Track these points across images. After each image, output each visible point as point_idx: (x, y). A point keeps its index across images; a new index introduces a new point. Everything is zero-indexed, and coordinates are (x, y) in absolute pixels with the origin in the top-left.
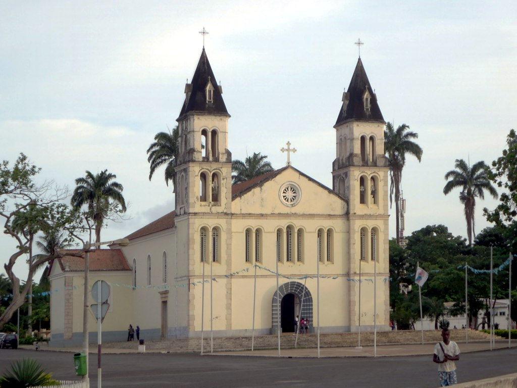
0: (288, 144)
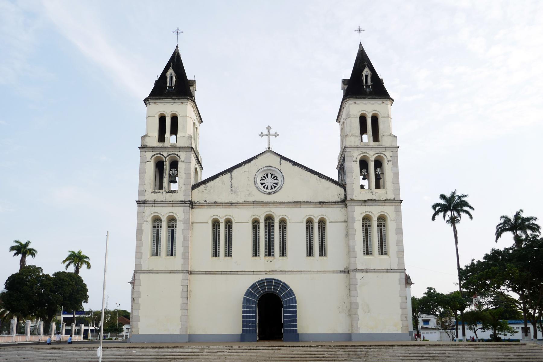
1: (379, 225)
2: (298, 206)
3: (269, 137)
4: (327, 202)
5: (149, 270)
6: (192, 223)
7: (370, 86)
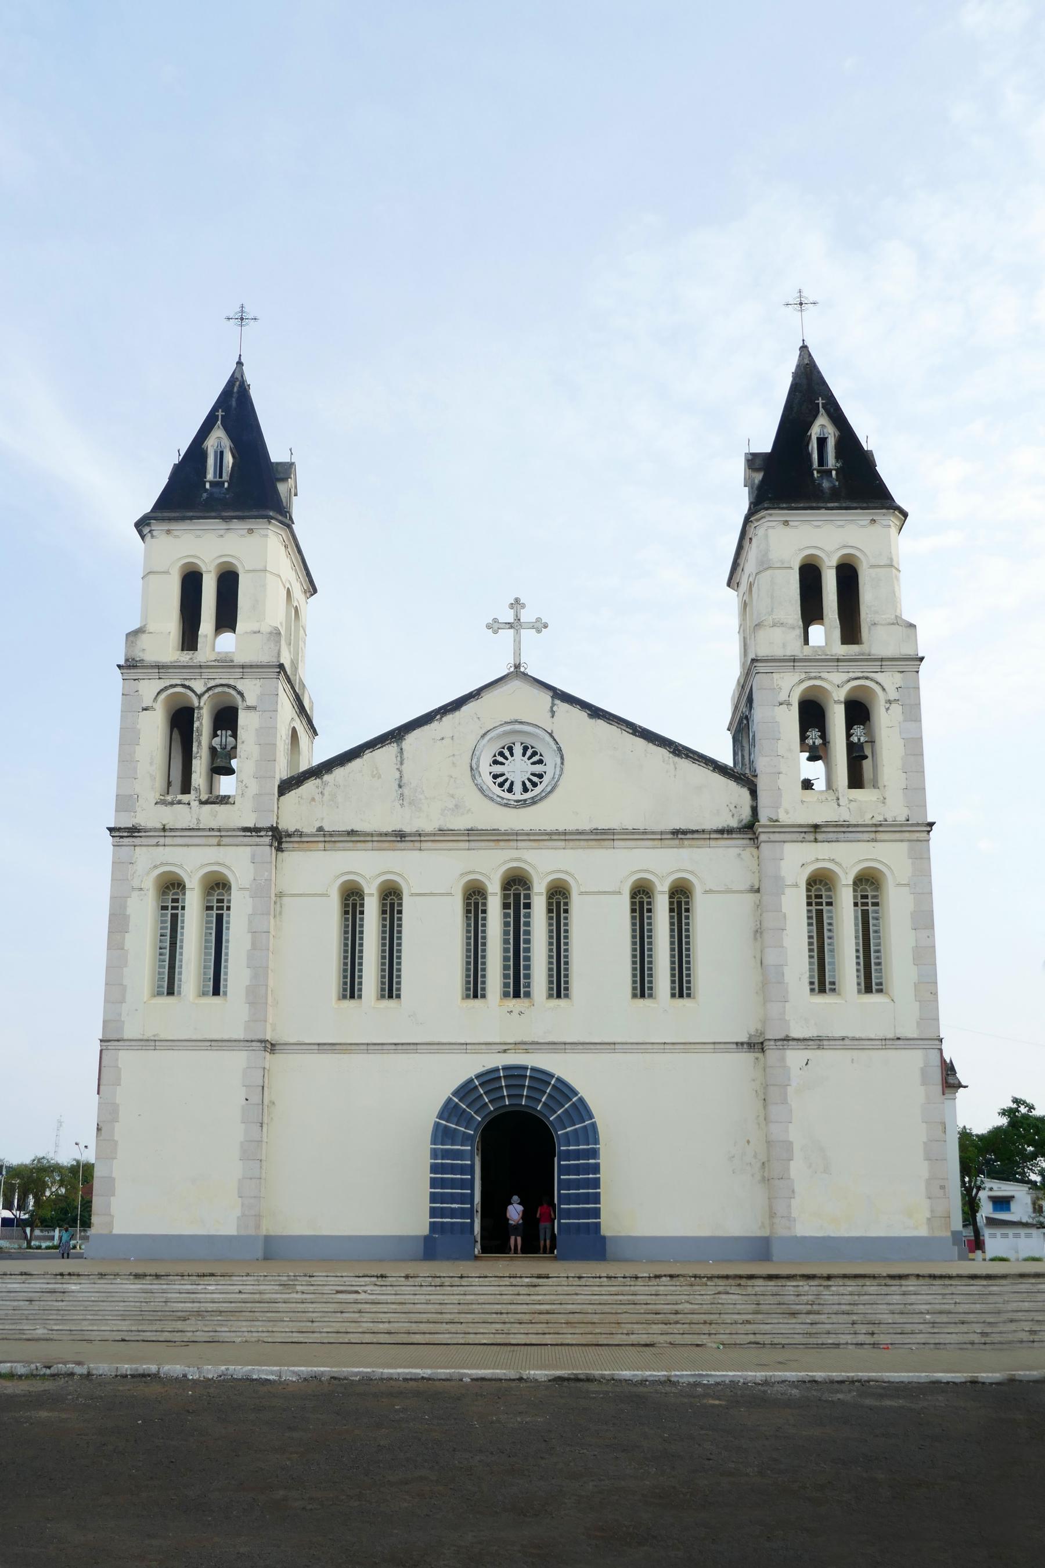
0: (517, 604)
1: (860, 901)
2: (606, 843)
3: (517, 632)
4: (697, 831)
5: (145, 1037)
6: (280, 895)
7: (834, 473)
